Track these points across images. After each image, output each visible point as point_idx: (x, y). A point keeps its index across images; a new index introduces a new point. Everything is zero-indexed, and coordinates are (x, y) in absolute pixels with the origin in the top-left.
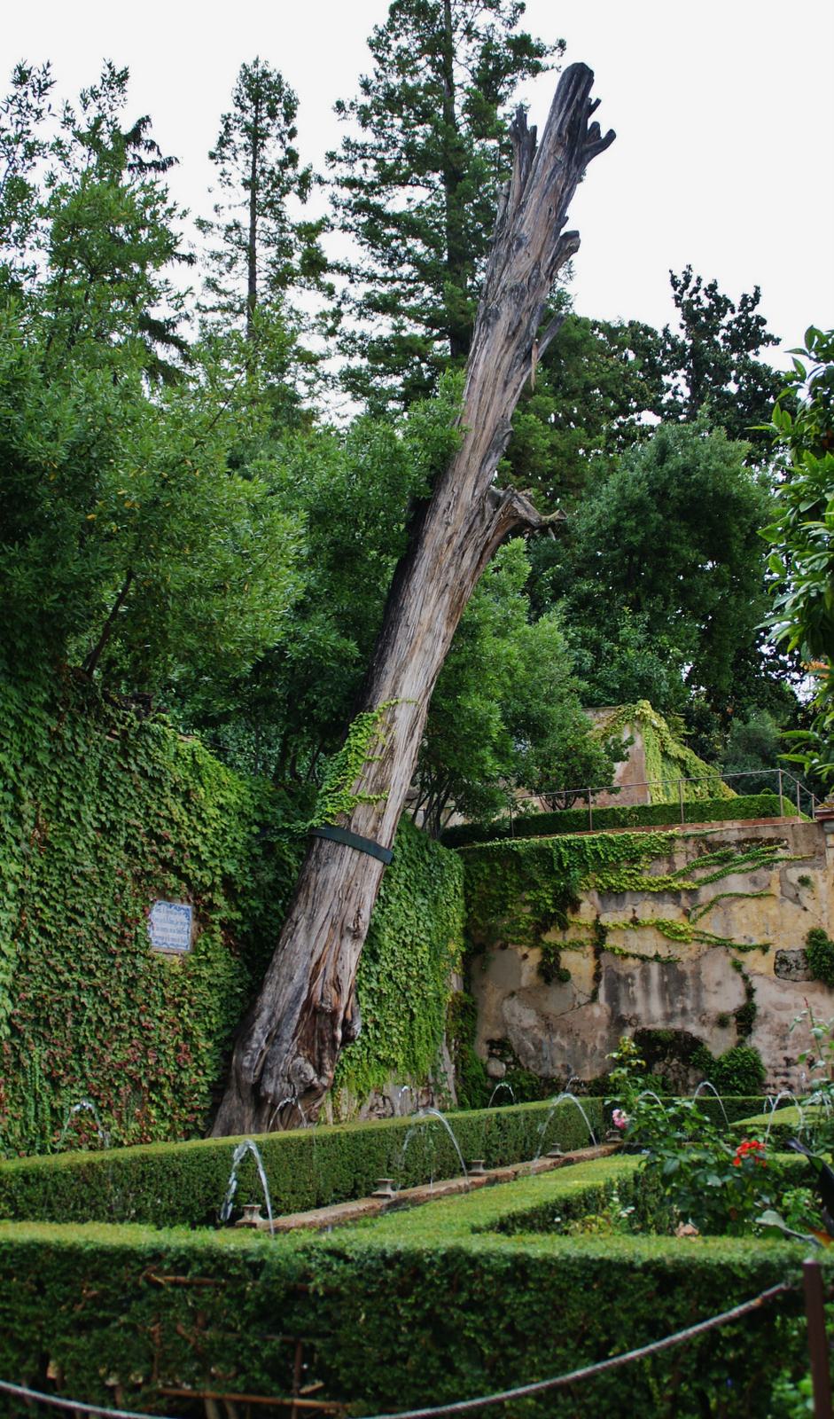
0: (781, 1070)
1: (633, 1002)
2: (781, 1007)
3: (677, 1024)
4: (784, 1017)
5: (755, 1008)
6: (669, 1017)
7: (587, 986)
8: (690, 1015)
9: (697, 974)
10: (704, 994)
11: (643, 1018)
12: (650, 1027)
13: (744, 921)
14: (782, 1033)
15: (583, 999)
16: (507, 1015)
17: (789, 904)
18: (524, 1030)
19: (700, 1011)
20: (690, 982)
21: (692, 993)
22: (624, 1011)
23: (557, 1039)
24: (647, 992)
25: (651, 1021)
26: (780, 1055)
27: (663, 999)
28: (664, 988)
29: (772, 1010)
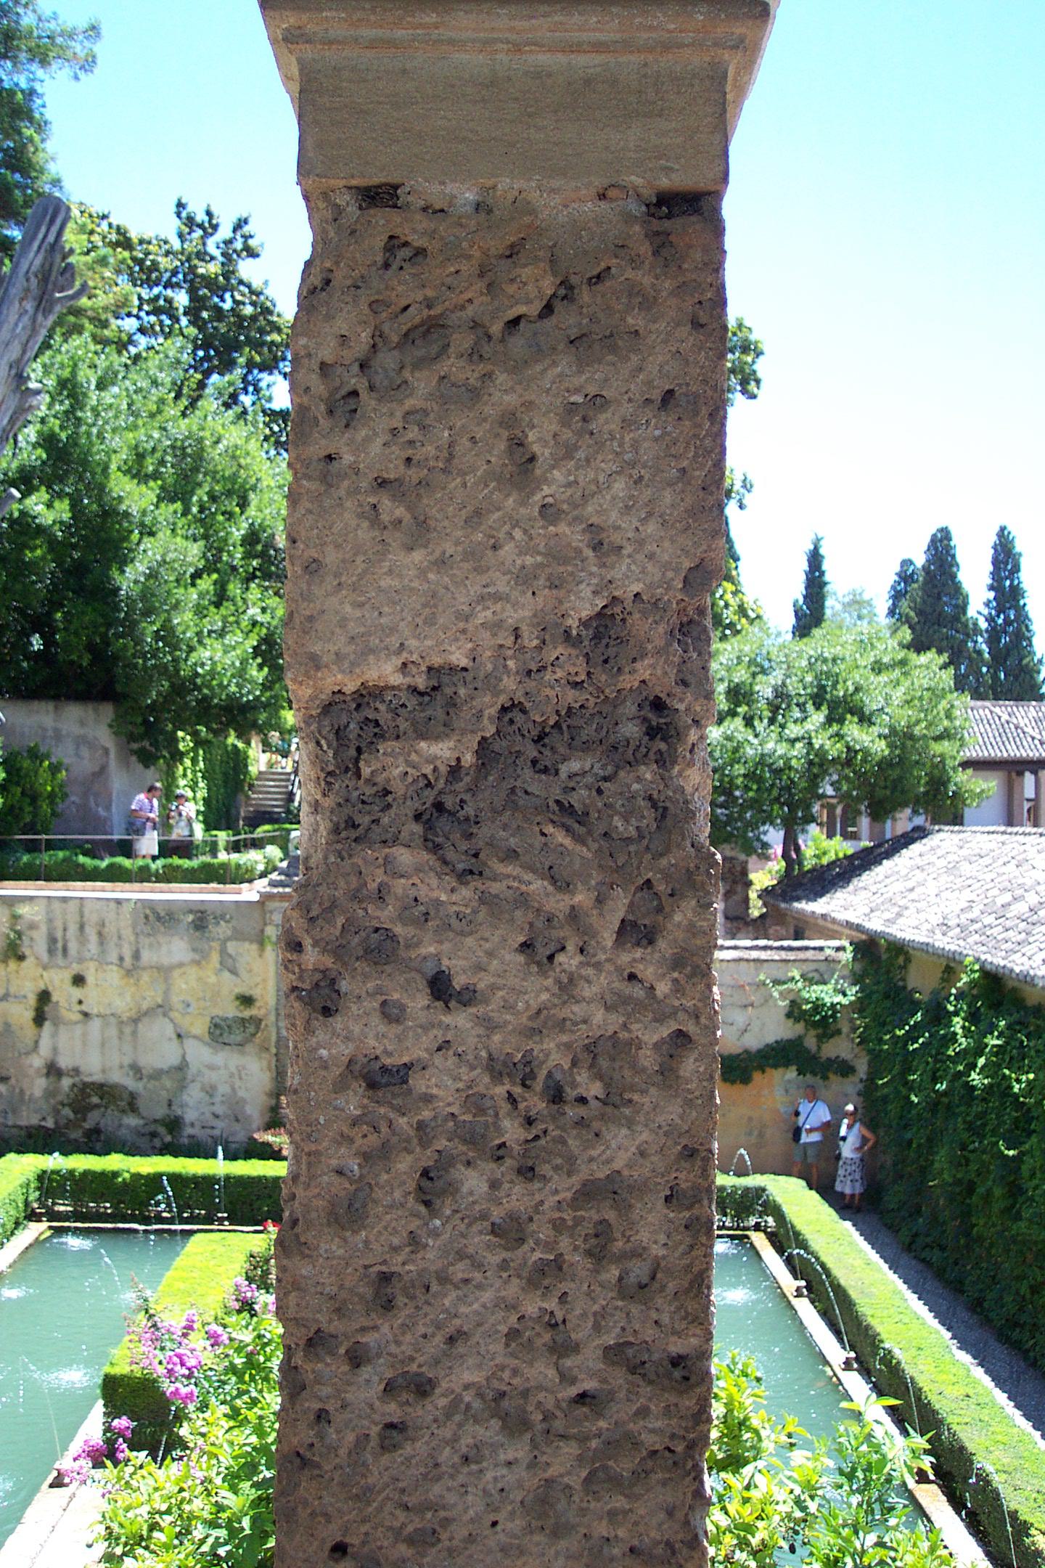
2: (212, 1067)
4: (212, 1077)
5: (187, 1065)
13: (184, 986)
14: (210, 1091)
17: (226, 974)
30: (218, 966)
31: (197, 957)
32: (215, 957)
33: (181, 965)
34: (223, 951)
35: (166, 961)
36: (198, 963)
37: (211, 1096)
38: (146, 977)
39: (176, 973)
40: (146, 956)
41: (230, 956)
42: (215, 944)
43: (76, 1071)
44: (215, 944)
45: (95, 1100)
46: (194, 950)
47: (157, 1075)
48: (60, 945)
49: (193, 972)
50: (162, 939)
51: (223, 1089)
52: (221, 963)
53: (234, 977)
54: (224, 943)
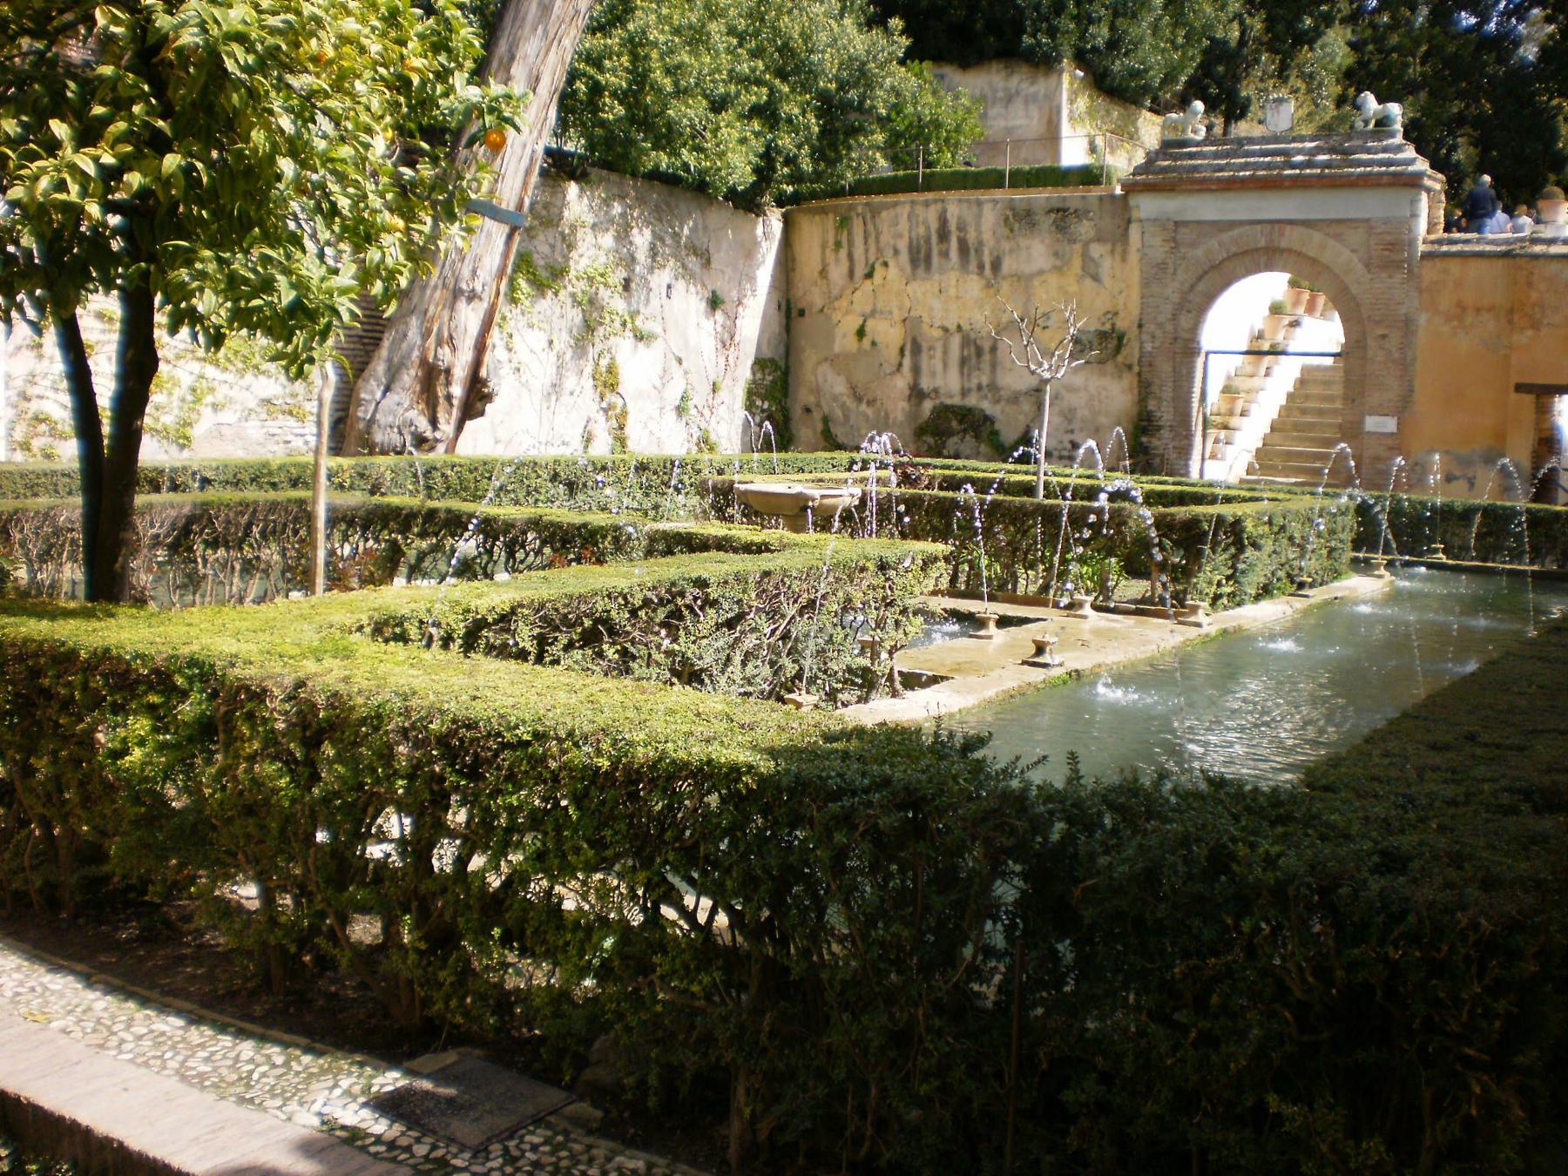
0: (1066, 453)
1: (933, 374)
3: (972, 401)
6: (964, 393)
7: (895, 352)
8: (986, 390)
9: (994, 349)
10: (999, 371)
11: (942, 391)
12: (949, 402)
15: (888, 369)
16: (820, 380)
17: (1088, 282)
18: (835, 398)
19: (993, 387)
20: (987, 357)
21: (986, 366)
22: (926, 384)
23: (863, 407)
24: (945, 365)
25: (951, 397)
26: (1067, 438)
27: (962, 373)
28: (963, 361)
29: (1063, 392)
30: (1079, 272)
31: (1058, 263)
32: (1077, 263)
33: (1041, 272)
34: (1085, 255)
35: (1027, 269)
36: (1058, 269)
37: (1070, 421)
38: (1005, 287)
39: (1036, 283)
40: (1007, 265)
41: (1093, 260)
42: (1078, 247)
43: (936, 391)
44: (1078, 247)
45: (954, 423)
46: (1056, 254)
47: (1015, 399)
48: (922, 255)
49: (1053, 280)
50: (1023, 242)
51: (1083, 413)
52: (1083, 268)
53: (1095, 284)
54: (1086, 245)
